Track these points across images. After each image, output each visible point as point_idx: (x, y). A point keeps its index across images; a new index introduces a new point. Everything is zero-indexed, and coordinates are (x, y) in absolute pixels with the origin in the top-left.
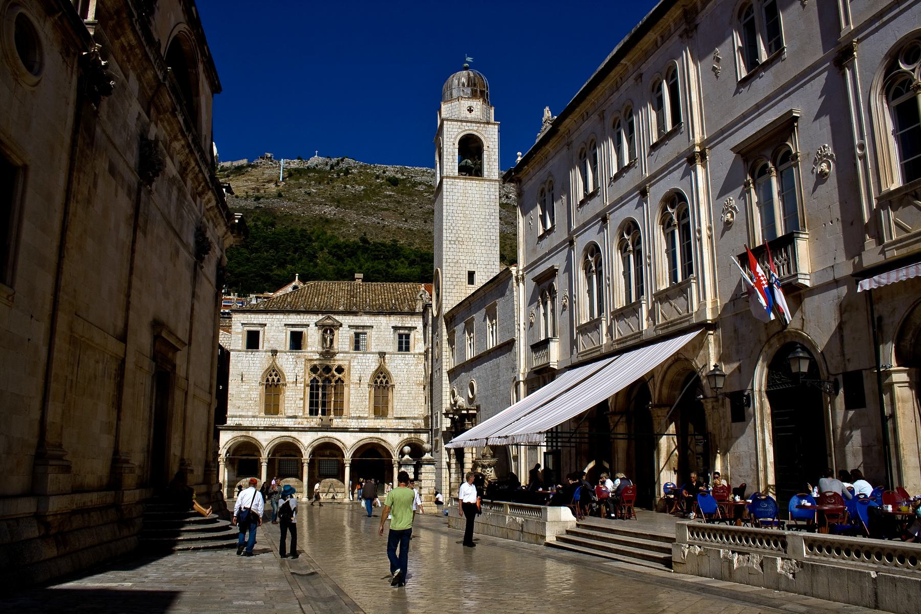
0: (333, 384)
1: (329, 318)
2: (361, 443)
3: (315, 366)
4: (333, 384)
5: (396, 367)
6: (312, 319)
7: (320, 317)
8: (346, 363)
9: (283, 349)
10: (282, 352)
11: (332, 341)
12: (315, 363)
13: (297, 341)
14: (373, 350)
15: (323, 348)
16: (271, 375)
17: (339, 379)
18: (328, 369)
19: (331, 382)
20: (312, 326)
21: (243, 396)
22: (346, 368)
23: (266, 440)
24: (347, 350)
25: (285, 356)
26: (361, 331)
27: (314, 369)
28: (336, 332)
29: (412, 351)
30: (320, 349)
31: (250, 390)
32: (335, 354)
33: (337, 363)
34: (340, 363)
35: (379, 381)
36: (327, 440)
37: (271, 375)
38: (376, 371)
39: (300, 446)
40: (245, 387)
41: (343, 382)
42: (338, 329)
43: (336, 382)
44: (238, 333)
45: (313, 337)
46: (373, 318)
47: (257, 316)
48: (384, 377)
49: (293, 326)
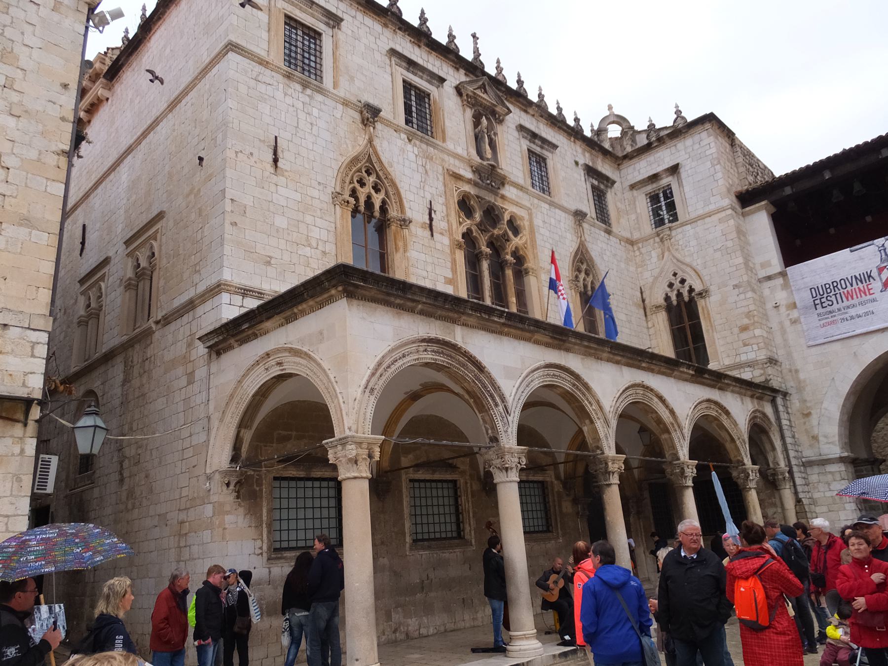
0: (509, 257)
2: (698, 415)
6: (454, 77)
10: (388, 123)
12: (467, 188)
14: (565, 205)
18: (492, 215)
20: (449, 87)
21: (281, 222)
23: (509, 373)
24: (521, 181)
26: (538, 150)
27: (465, 205)
36: (638, 395)
37: (362, 183)
39: (591, 409)
40: (285, 193)
49: (411, 64)
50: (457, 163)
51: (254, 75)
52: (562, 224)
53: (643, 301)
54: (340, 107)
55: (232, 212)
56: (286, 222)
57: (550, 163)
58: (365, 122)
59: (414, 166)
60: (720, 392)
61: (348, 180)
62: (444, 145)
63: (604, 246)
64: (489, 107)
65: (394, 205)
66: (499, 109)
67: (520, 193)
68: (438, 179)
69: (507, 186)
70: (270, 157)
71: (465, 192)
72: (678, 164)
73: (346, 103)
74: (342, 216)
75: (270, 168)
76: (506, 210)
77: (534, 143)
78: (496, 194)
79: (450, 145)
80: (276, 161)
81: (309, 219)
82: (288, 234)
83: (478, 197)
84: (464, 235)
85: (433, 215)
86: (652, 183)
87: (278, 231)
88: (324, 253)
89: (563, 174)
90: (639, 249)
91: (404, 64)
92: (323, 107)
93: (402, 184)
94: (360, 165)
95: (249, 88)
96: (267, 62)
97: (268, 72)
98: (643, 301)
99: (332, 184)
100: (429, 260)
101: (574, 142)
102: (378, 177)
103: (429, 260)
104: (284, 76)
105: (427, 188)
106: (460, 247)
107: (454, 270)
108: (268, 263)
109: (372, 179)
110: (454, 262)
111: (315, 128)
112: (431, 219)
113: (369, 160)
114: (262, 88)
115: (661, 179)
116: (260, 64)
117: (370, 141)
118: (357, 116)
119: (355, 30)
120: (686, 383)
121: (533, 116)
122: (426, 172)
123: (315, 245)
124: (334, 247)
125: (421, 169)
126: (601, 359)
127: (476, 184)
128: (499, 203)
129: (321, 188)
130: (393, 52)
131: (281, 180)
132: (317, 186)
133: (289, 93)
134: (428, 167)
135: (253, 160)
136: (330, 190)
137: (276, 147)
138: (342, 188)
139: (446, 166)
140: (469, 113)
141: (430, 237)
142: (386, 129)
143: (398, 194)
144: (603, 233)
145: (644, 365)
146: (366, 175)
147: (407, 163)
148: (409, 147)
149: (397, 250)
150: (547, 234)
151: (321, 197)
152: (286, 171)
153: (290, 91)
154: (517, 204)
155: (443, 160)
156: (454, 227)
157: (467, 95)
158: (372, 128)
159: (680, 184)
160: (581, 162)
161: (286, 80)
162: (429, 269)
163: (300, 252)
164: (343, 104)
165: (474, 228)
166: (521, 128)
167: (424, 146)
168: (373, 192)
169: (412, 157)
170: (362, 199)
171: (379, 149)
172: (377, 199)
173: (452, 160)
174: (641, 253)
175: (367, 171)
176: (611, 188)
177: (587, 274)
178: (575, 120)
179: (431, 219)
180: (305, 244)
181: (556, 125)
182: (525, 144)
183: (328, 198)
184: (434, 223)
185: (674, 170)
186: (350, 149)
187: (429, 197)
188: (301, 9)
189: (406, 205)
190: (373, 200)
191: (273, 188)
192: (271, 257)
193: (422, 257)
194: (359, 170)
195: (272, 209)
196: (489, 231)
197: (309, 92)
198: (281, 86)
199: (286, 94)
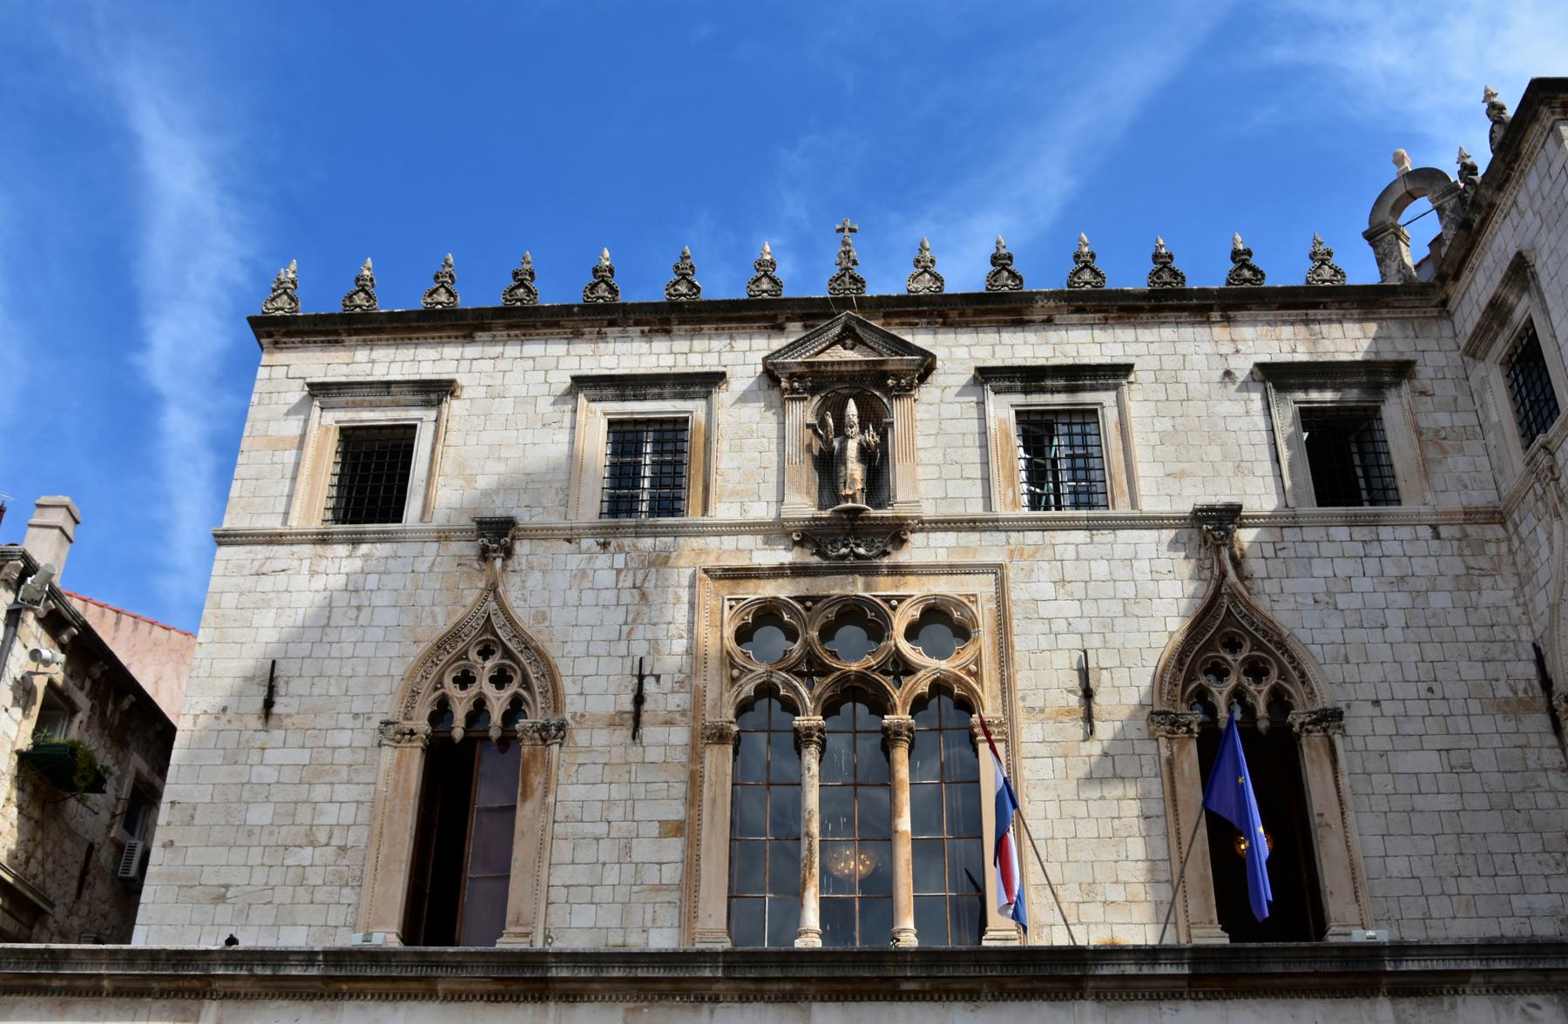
1: (849, 337)
3: (767, 613)
4: (900, 717)
5: (1325, 602)
7: (795, 331)
8: (982, 586)
9: (554, 520)
10: (544, 534)
11: (876, 463)
13: (651, 471)
15: (821, 507)
16: (465, 680)
17: (940, 687)
19: (881, 705)
21: (260, 815)
22: (984, 615)
24: (976, 509)
25: (569, 559)
28: (899, 411)
29: (1415, 497)
30: (803, 505)
31: (315, 772)
32: (896, 532)
33: (919, 589)
34: (942, 587)
35: (1221, 695)
37: (465, 680)
38: (1197, 627)
40: (282, 754)
41: (966, 705)
42: (904, 391)
43: (918, 705)
44: (275, 444)
45: (752, 460)
46: (1126, 333)
47: (406, 353)
48: (1256, 670)
50: (746, 541)
51: (257, 564)
52: (1143, 566)
53: (1546, 683)
54: (432, 548)
55: (169, 824)
56: (270, 813)
57: (1110, 416)
58: (484, 555)
59: (610, 597)
60: (1408, 1005)
61: (426, 686)
62: (706, 520)
63: (1344, 567)
64: (863, 374)
65: (539, 699)
66: (894, 362)
67: (974, 537)
68: (678, 600)
69: (916, 539)
70: (258, 703)
71: (765, 600)
72: (1519, 255)
73: (443, 536)
74: (398, 764)
75: (259, 724)
76: (901, 599)
77: (1042, 390)
78: (871, 571)
79: (723, 511)
80: (269, 704)
81: (321, 792)
82: (271, 833)
83: (801, 600)
84: (743, 708)
85: (649, 686)
86: (1502, 325)
87: (250, 833)
88: (343, 849)
89: (1165, 425)
90: (1516, 526)
91: (609, 392)
92: (392, 564)
93: (568, 647)
94: (460, 645)
95: (241, 594)
96: (281, 535)
97: (282, 551)
98: (1546, 683)
99: (389, 707)
100: (618, 792)
101: (1228, 321)
102: (507, 653)
103: (618, 792)
104: (314, 543)
105: (639, 632)
106: (720, 736)
107: (693, 797)
108: (221, 899)
109: (489, 664)
110: (695, 781)
111: (366, 612)
112: (639, 699)
113: (488, 625)
114: (267, 583)
115: (1511, 310)
116: (270, 543)
117: (493, 589)
118: (470, 549)
119: (498, 382)
120: (1166, 1006)
121: (1049, 321)
122: (644, 596)
123: (323, 839)
124: (365, 832)
125: (626, 597)
126: (715, 999)
127: (797, 571)
128: (885, 587)
129: (358, 723)
130: (581, 383)
131: (278, 734)
132: (350, 723)
133: (321, 569)
134: (650, 585)
135: (224, 719)
136: (375, 723)
137: (272, 679)
138: (410, 706)
139: (711, 562)
140: (802, 413)
141: (629, 740)
142: (541, 547)
143: (550, 674)
144: (1341, 533)
145: (905, 986)
146: (479, 660)
147: (588, 597)
148: (603, 560)
149: (525, 797)
150: (1072, 609)
151: (351, 738)
152: (289, 716)
153: (323, 565)
154: (951, 570)
155: (701, 552)
156: (711, 695)
157: (791, 377)
158: (499, 563)
159: (1546, 311)
160: (1243, 367)
161: (319, 549)
162: (616, 814)
163: (287, 862)
164: (439, 540)
165: (780, 678)
166: (987, 376)
167: (647, 543)
168: (490, 690)
169: (606, 578)
170: (460, 712)
171: (512, 595)
172: (498, 702)
173: (729, 542)
174: (1522, 542)
175: (492, 646)
176: (1398, 385)
177: (1256, 670)
178: (1233, 259)
179: (639, 699)
180: (301, 840)
181: (1140, 310)
182: (1002, 410)
183: (366, 738)
184: (647, 706)
185: (1521, 271)
186: (441, 619)
187: (640, 649)
188: (372, 406)
189: (568, 687)
190: (489, 706)
191: (255, 756)
192: (227, 887)
193: (602, 791)
194: (463, 655)
195: (246, 795)
196: (831, 670)
197: (364, 548)
198: (306, 563)
199: (313, 573)
